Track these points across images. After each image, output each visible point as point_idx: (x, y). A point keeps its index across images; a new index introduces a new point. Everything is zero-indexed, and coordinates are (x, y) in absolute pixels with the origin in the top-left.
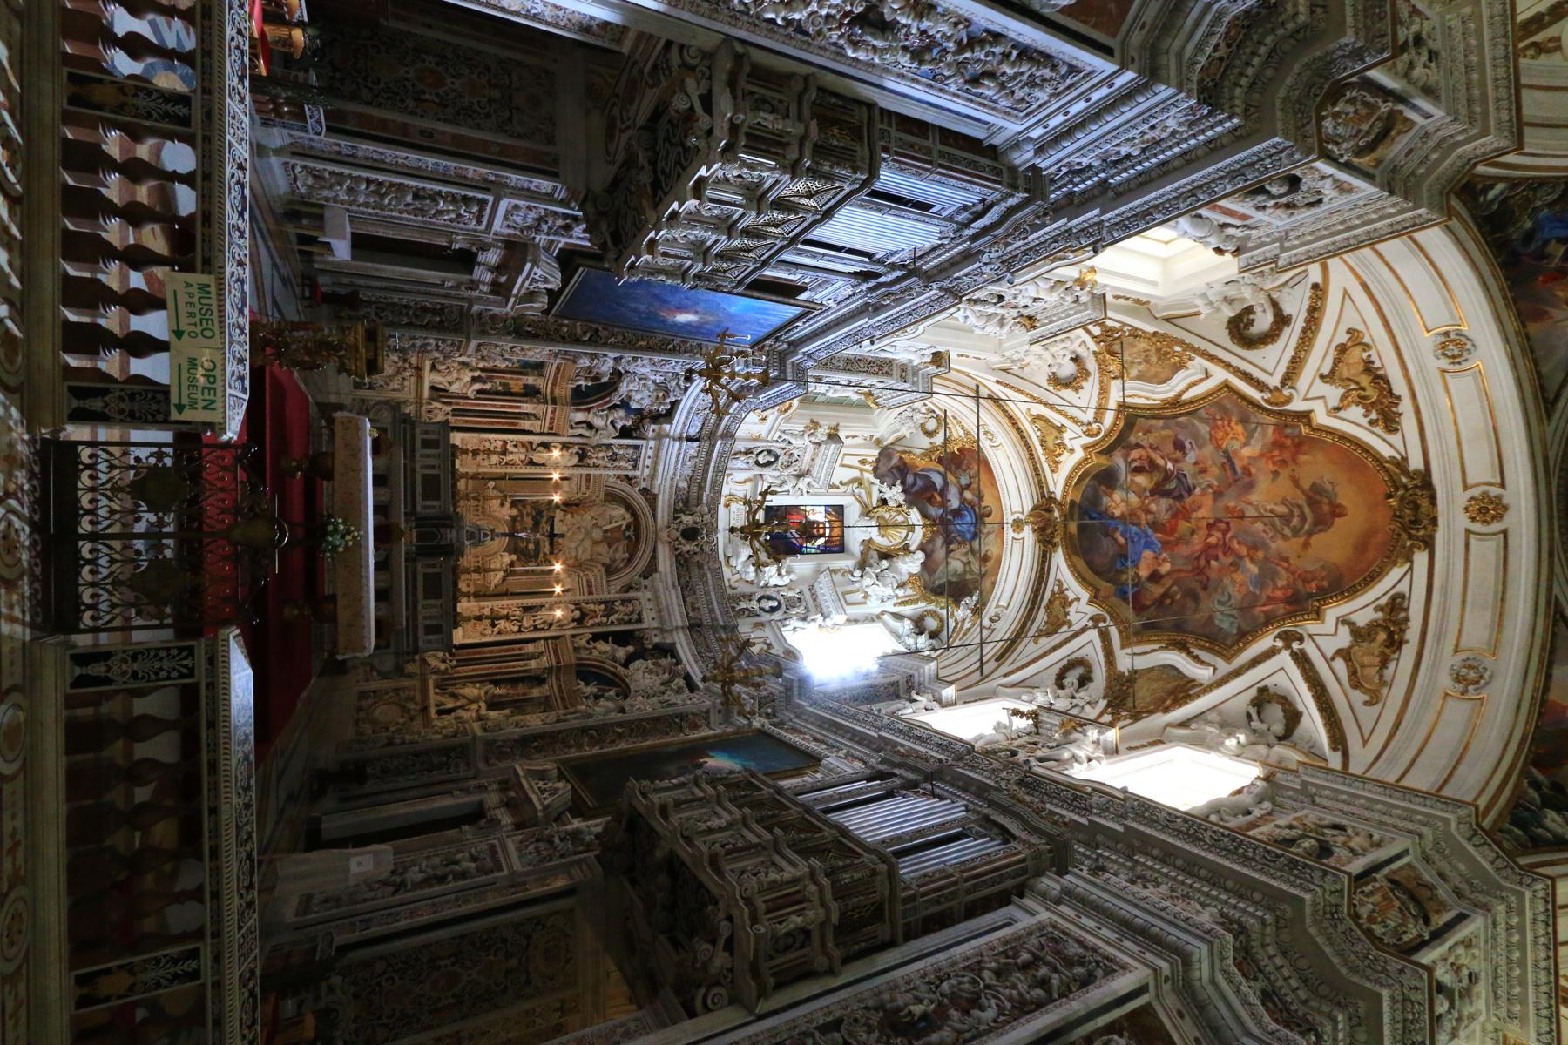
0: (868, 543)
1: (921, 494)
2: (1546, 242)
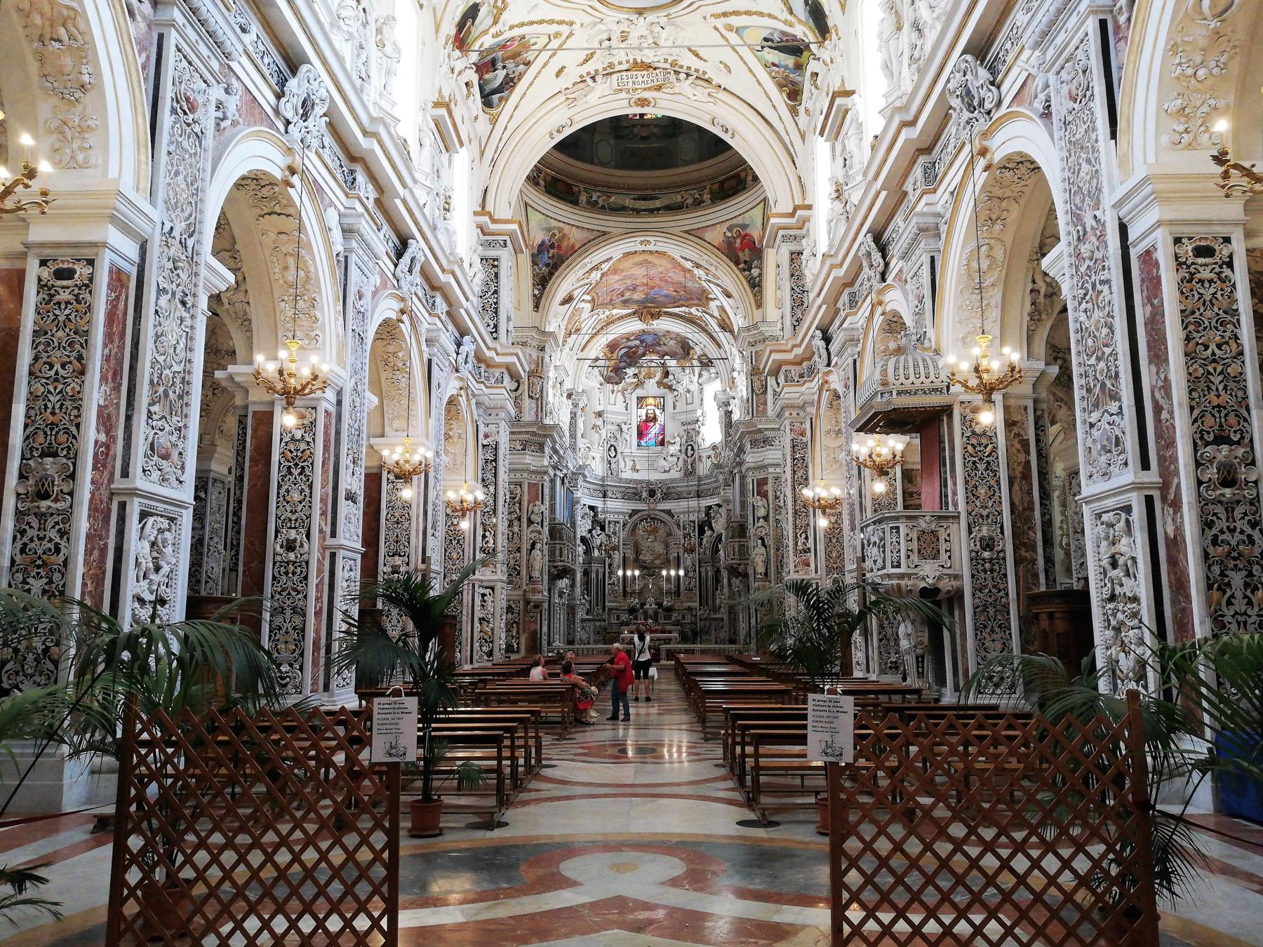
0: (659, 384)
1: (632, 358)
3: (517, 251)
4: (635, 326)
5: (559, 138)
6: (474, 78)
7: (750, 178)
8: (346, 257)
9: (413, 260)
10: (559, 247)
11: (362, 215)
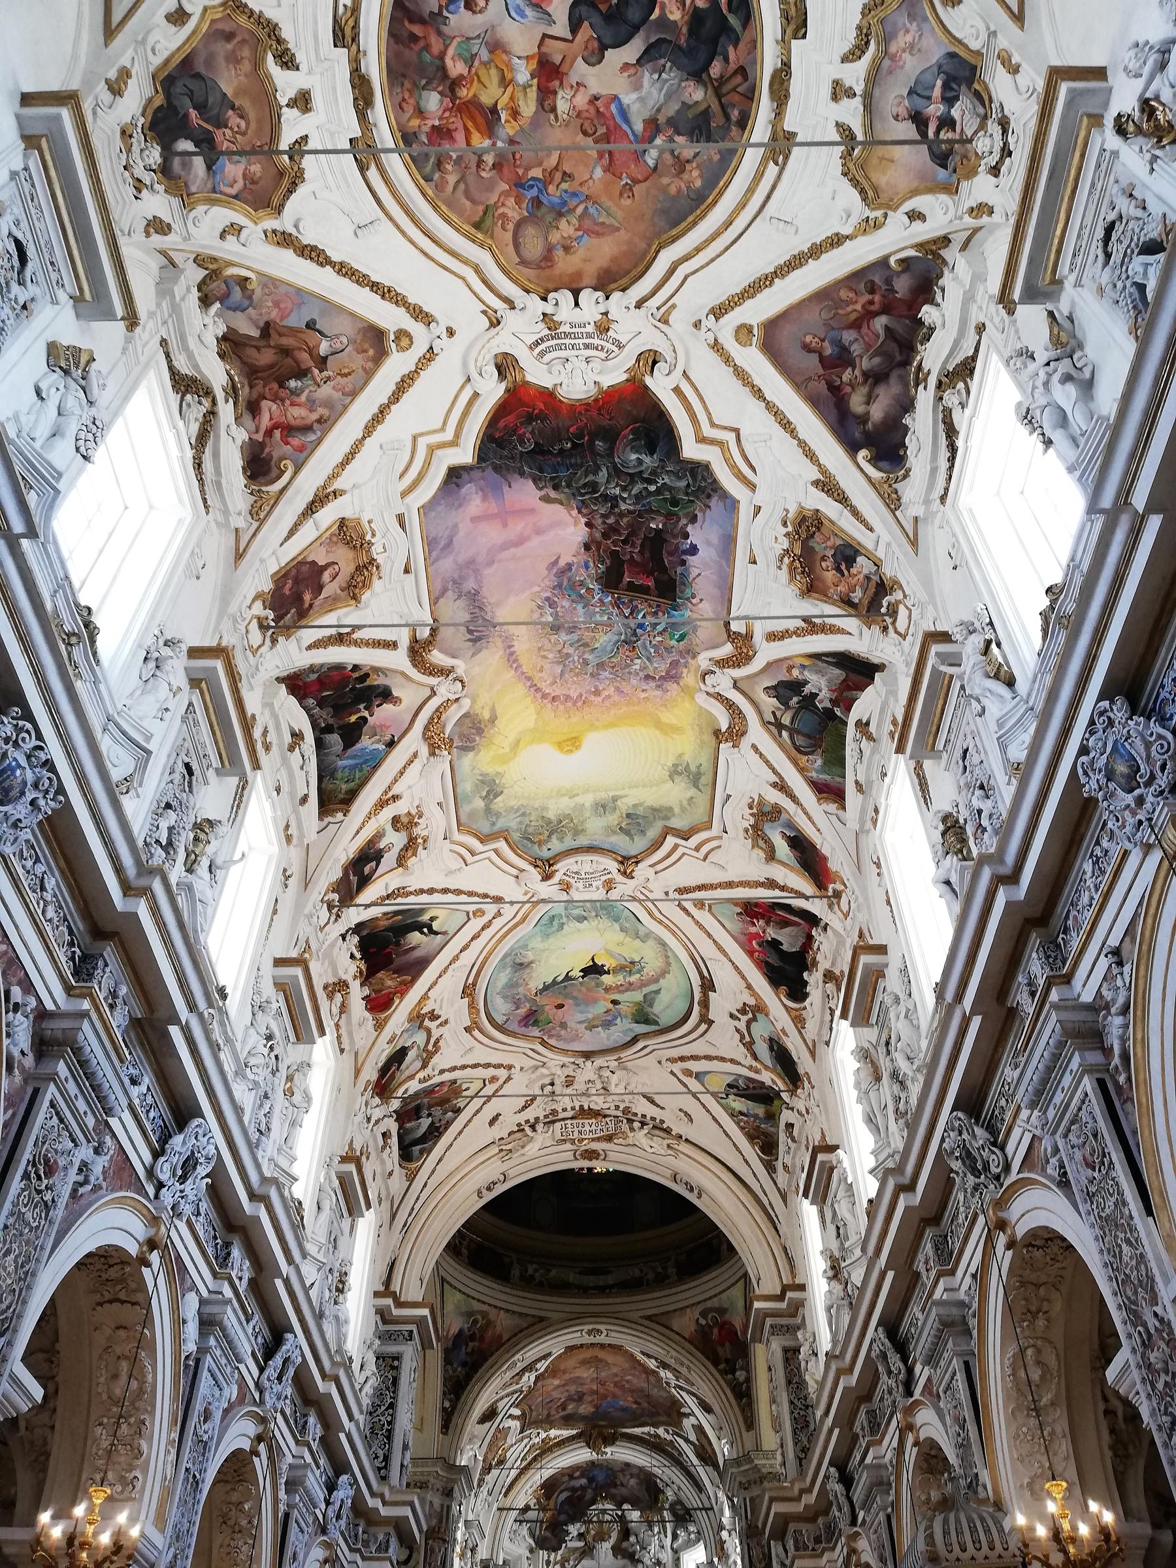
0: (617, 1550)
3: (426, 1345)
4: (582, 1455)
5: (489, 1197)
6: (392, 1126)
7: (725, 1246)
8: (198, 1361)
9: (286, 1361)
10: (482, 1339)
11: (229, 1301)
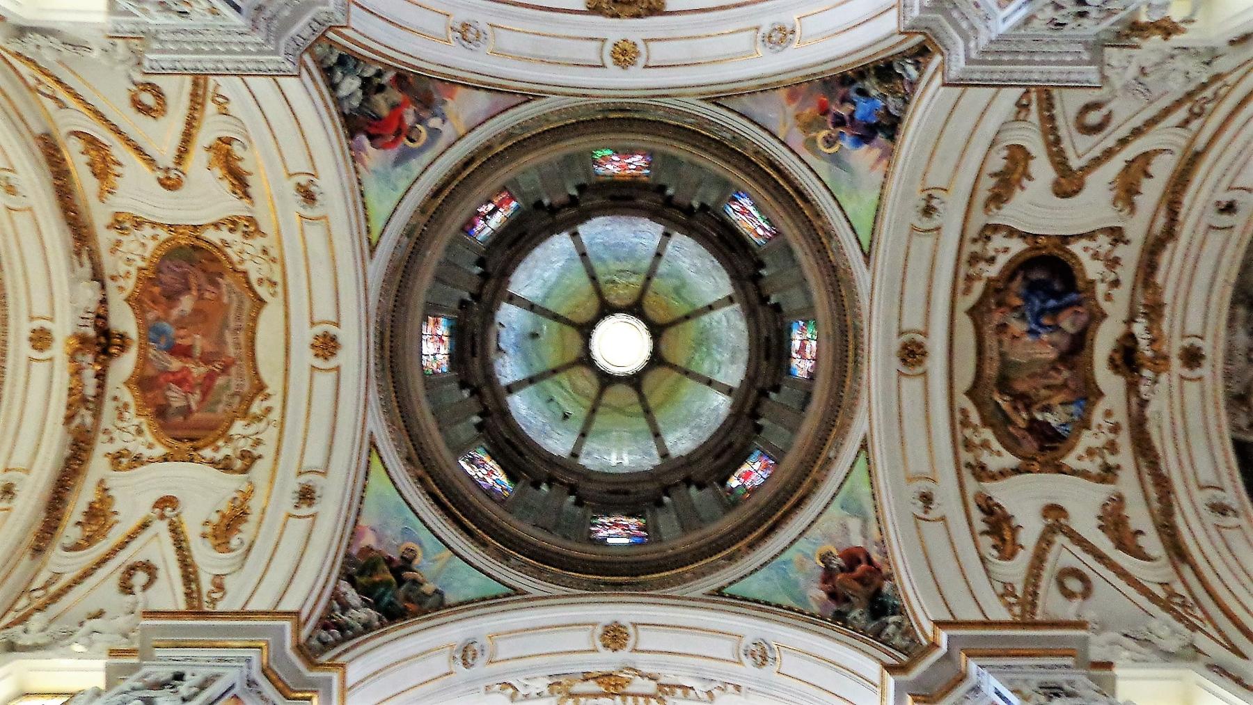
2: (854, 104)
